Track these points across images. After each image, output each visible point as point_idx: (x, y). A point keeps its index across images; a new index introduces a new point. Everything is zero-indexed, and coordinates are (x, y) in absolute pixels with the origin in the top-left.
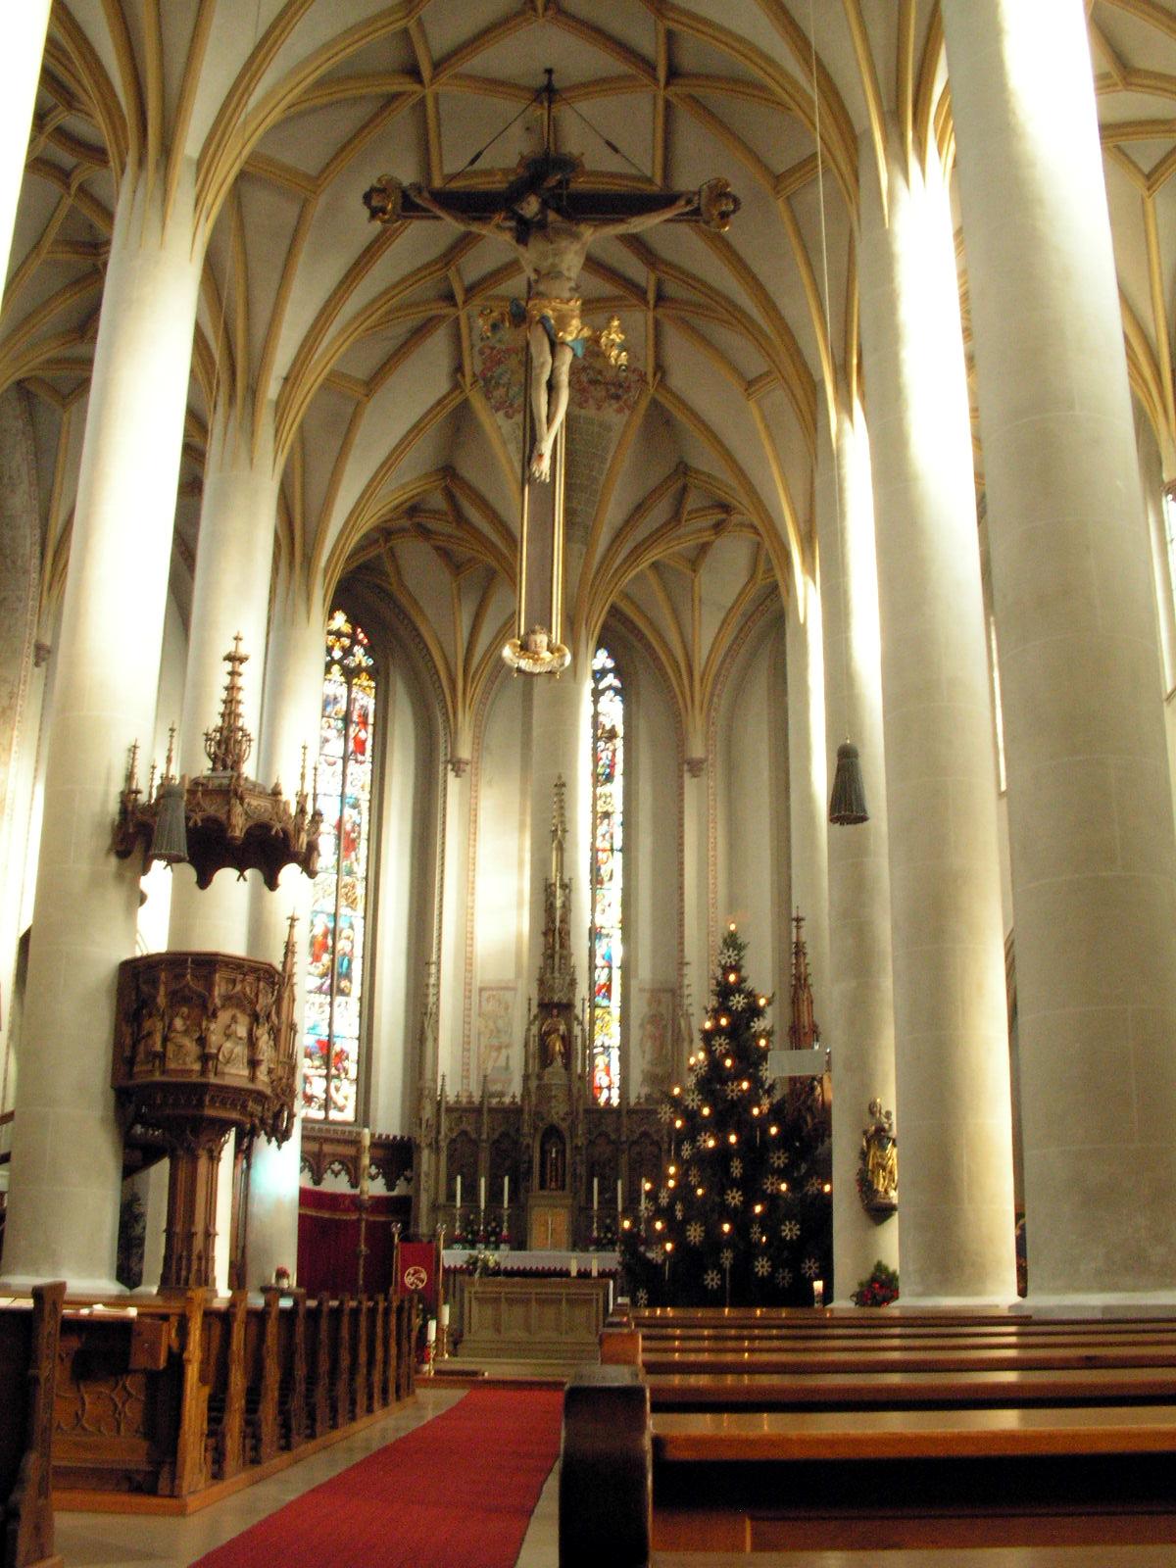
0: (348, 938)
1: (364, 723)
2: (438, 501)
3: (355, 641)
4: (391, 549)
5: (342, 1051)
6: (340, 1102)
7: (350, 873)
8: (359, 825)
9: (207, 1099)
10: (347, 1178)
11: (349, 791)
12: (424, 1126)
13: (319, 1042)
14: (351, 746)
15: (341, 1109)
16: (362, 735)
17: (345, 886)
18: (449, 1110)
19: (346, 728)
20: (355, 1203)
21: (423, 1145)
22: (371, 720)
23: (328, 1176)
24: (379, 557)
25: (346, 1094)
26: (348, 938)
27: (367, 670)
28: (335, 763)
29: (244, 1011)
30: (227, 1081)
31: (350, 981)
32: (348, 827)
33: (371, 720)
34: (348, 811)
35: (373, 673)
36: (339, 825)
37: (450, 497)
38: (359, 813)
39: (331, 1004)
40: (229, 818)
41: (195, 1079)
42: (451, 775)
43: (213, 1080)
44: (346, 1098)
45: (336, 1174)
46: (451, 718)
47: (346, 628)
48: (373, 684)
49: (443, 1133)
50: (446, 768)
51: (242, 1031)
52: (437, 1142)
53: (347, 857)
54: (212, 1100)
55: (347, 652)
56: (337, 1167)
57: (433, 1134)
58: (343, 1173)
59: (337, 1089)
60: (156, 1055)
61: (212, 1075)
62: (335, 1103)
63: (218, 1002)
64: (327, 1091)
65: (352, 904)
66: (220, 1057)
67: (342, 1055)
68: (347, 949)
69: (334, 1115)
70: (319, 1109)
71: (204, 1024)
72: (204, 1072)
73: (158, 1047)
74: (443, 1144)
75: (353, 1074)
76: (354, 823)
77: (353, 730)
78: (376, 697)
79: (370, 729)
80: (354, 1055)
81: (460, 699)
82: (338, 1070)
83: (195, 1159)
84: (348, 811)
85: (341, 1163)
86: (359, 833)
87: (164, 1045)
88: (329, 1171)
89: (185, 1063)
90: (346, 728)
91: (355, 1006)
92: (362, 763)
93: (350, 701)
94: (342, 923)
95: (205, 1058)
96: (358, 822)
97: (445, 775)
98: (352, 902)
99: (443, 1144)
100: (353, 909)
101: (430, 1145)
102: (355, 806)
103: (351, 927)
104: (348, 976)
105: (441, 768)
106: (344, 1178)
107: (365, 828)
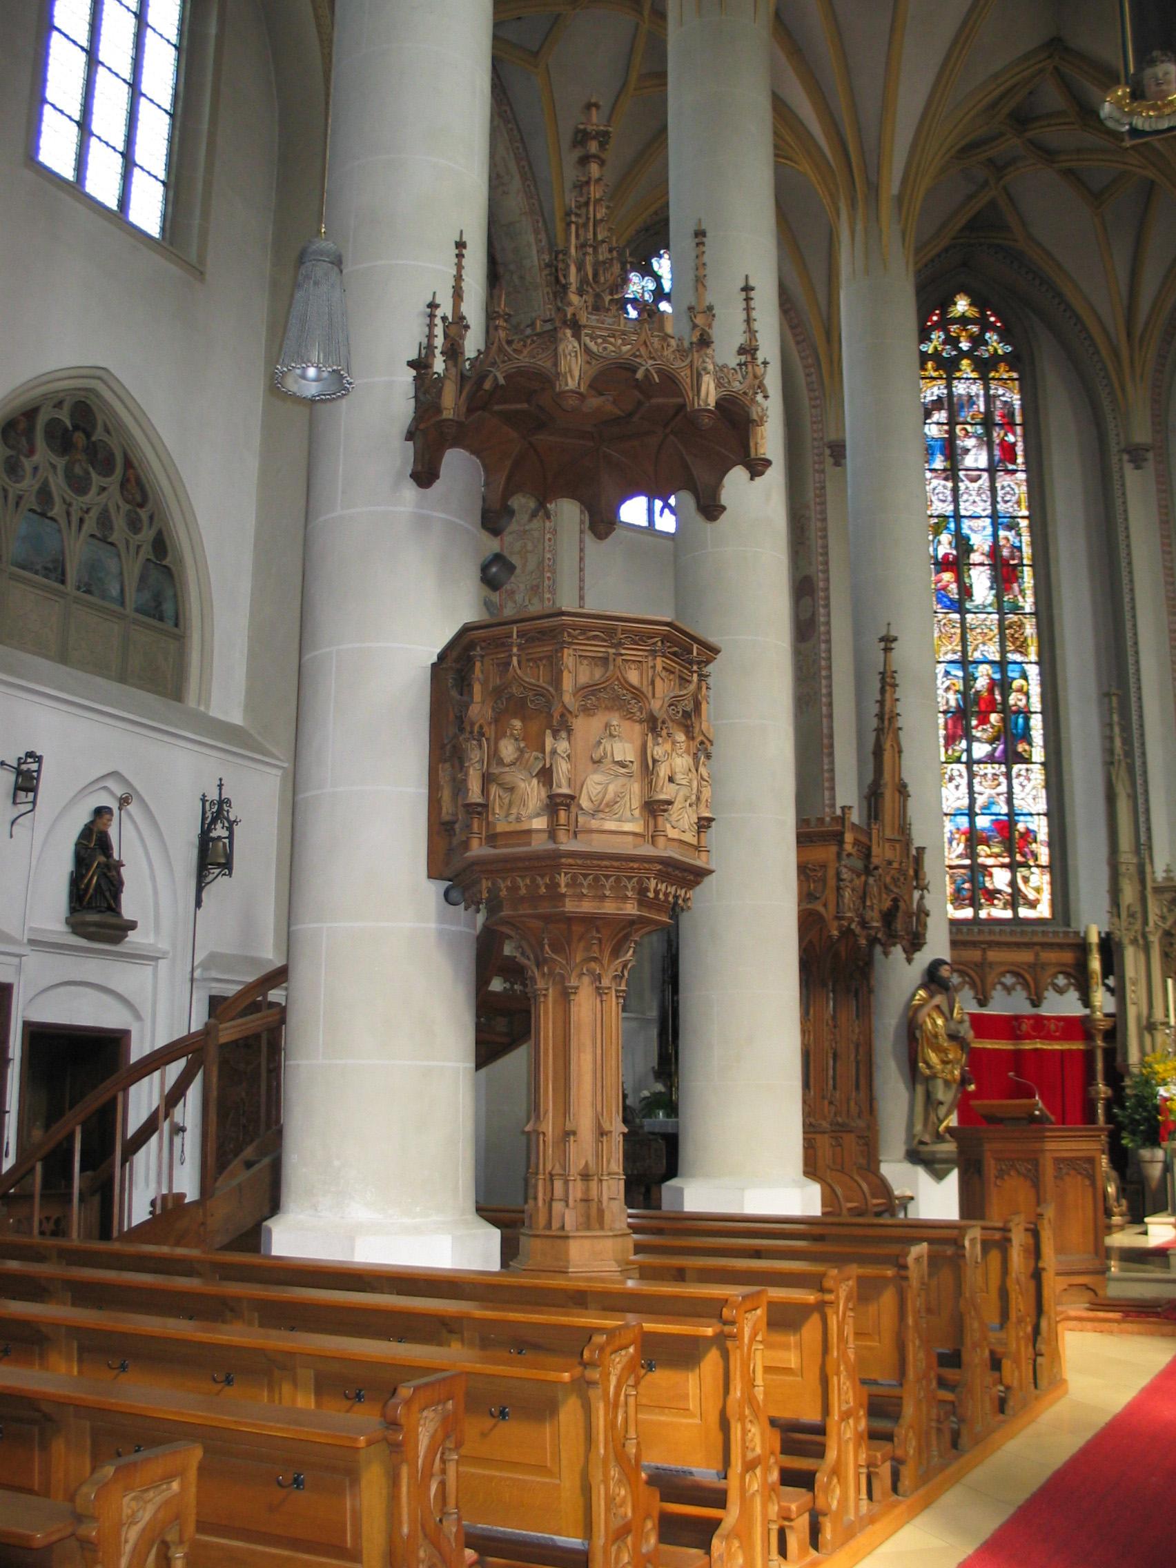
0: (1020, 690)
1: (1009, 425)
2: (1052, 98)
3: (986, 326)
4: (1005, 188)
5: (1028, 831)
6: (1032, 895)
7: (1016, 609)
8: (1020, 549)
9: (563, 880)
10: (1024, 994)
11: (1001, 507)
12: (1124, 914)
13: (996, 822)
14: (997, 452)
15: (1033, 905)
16: (1011, 438)
17: (1010, 627)
18: (1158, 890)
19: (988, 433)
20: (1040, 1026)
21: (1126, 941)
22: (1018, 420)
23: (998, 994)
24: (993, 204)
25: (1038, 883)
26: (1020, 690)
27: (1005, 358)
28: (979, 477)
29: (629, 716)
30: (597, 844)
31: (1030, 744)
32: (1006, 553)
33: (1018, 420)
34: (1002, 533)
35: (1013, 361)
36: (994, 551)
37: (1067, 86)
38: (1020, 535)
39: (1008, 776)
40: (556, 364)
41: (540, 844)
42: (1128, 468)
43: (567, 844)
44: (1038, 890)
45: (1009, 990)
46: (1119, 393)
47: (972, 313)
48: (1015, 375)
49: (1151, 923)
50: (1120, 460)
51: (624, 750)
52: (1144, 936)
53: (1008, 589)
54: (573, 883)
55: (978, 341)
56: (1009, 980)
57: (1138, 926)
58: (1019, 987)
59: (1026, 880)
60: (471, 809)
61: (562, 835)
62: (1025, 897)
63: (568, 698)
64: (1013, 883)
65: (1022, 648)
66: (584, 803)
67: (1029, 836)
68: (1022, 704)
69: (1024, 912)
70: (1005, 908)
71: (549, 741)
72: (552, 833)
73: (475, 795)
74: (1155, 939)
75: (1044, 859)
76: (1013, 546)
77: (997, 434)
78: (1021, 391)
79: (1019, 430)
80: (1043, 835)
81: (1127, 371)
82: (1024, 855)
83: (566, 995)
84: (1002, 533)
85: (1016, 974)
86: (1021, 558)
87: (485, 791)
88: (999, 987)
89: (518, 820)
90: (988, 433)
91: (1038, 774)
92: (1014, 472)
93: (989, 399)
94: (1013, 672)
95: (556, 805)
96: (1018, 544)
97: (1121, 468)
98: (1021, 646)
99: (1155, 939)
100: (1025, 654)
101: (1134, 942)
102: (1012, 526)
103: (1024, 676)
104: (1026, 737)
105: (1114, 459)
106: (1020, 995)
107: (1027, 551)
